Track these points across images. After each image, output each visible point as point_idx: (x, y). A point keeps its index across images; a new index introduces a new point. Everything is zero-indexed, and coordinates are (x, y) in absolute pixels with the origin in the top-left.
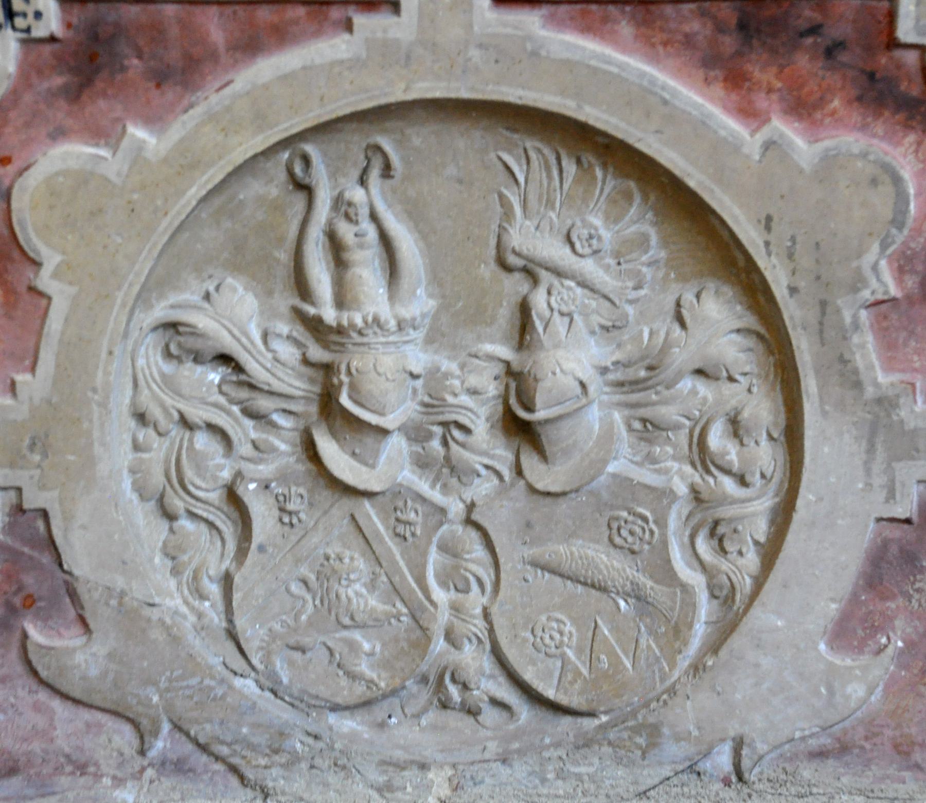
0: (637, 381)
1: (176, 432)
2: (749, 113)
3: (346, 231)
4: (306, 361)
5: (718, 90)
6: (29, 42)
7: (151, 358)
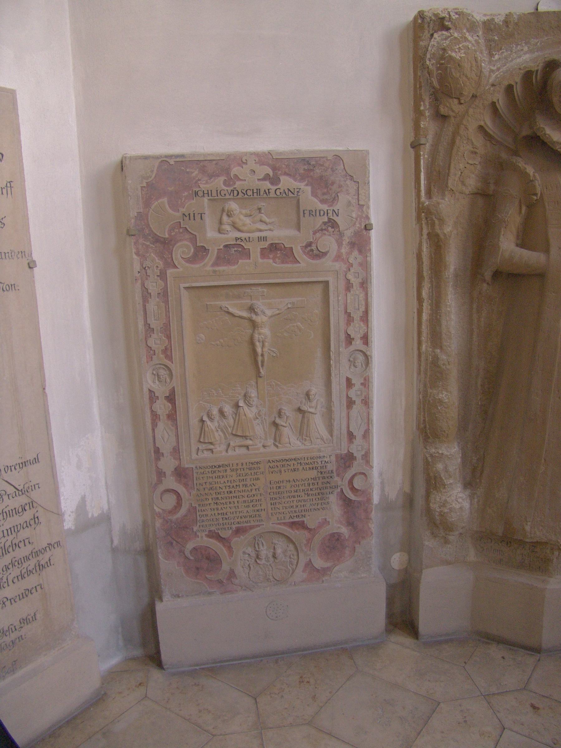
0: (285, 552)
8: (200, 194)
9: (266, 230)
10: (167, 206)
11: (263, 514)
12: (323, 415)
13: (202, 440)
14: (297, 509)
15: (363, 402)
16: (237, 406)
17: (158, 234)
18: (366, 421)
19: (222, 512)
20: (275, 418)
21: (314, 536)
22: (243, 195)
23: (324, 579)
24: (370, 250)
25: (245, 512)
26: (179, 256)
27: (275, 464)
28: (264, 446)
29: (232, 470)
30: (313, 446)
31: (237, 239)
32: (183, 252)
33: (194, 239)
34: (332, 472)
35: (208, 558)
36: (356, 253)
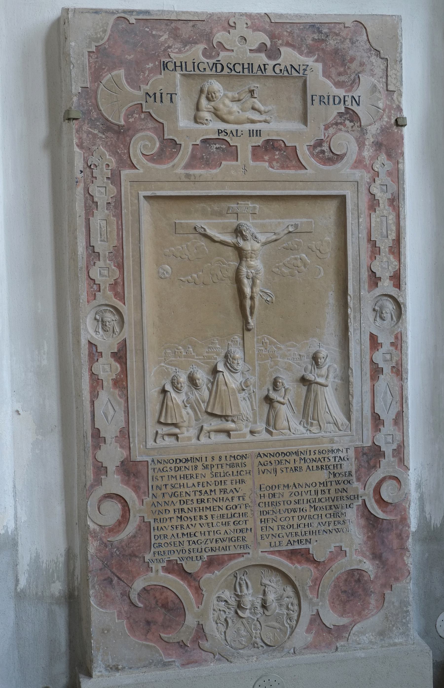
0: (279, 599)
1: (218, 612)
2: (292, 563)
3: (242, 582)
4: (236, 600)
5: (289, 561)
6: (203, 561)
7: (215, 602)
8: (171, 66)
9: (260, 122)
10: (124, 81)
11: (249, 536)
12: (336, 389)
13: (162, 420)
14: (299, 531)
15: (394, 370)
16: (215, 371)
17: (110, 119)
18: (398, 398)
19: (188, 531)
20: (268, 390)
21: (323, 574)
22: (229, 71)
23: (338, 645)
24: (402, 154)
25: (223, 532)
26: (138, 151)
27: (268, 459)
28: (252, 432)
29: (206, 467)
30: (323, 434)
31: (220, 132)
32: (145, 146)
33: (160, 128)
34: (350, 474)
35: (165, 606)
36: (383, 157)
